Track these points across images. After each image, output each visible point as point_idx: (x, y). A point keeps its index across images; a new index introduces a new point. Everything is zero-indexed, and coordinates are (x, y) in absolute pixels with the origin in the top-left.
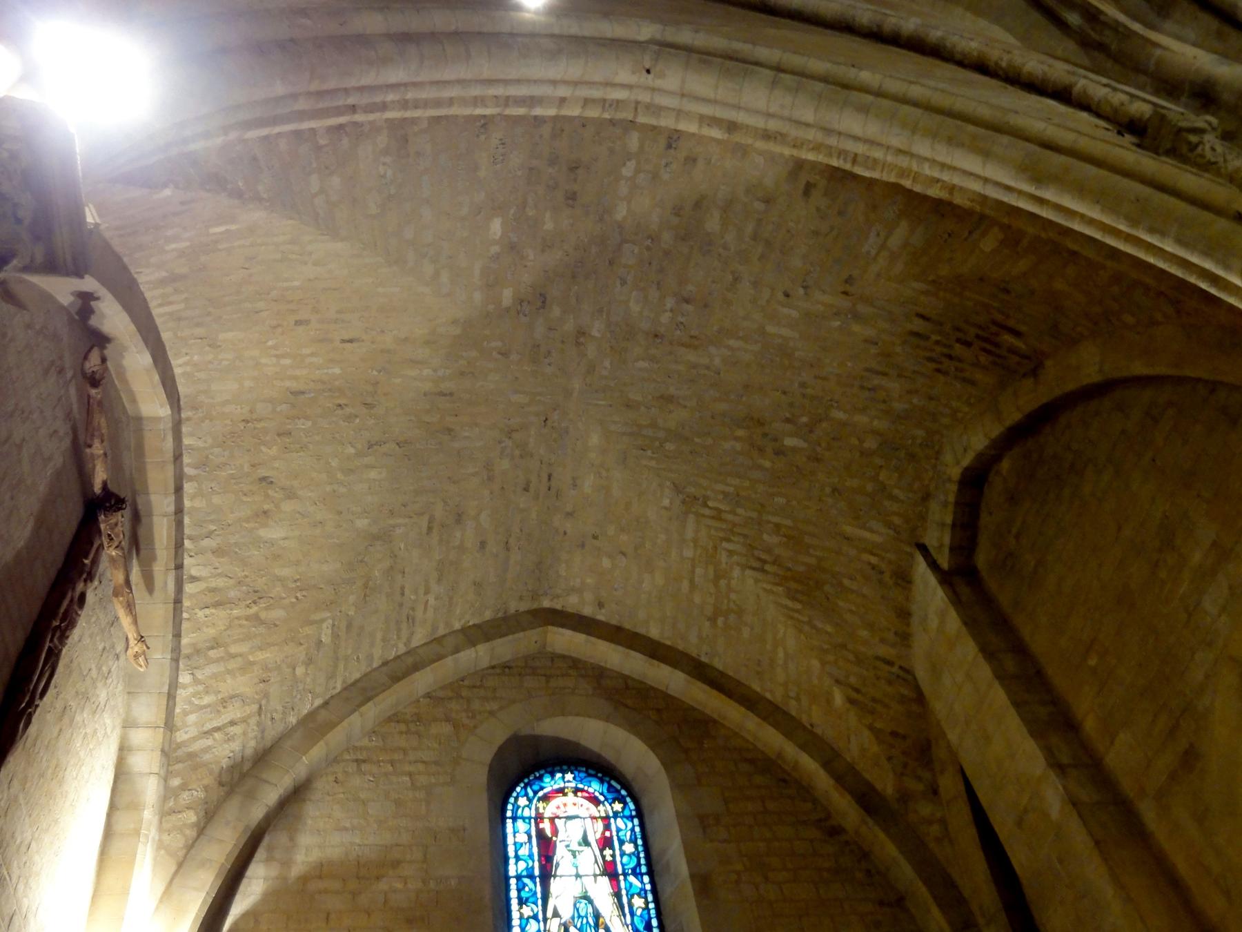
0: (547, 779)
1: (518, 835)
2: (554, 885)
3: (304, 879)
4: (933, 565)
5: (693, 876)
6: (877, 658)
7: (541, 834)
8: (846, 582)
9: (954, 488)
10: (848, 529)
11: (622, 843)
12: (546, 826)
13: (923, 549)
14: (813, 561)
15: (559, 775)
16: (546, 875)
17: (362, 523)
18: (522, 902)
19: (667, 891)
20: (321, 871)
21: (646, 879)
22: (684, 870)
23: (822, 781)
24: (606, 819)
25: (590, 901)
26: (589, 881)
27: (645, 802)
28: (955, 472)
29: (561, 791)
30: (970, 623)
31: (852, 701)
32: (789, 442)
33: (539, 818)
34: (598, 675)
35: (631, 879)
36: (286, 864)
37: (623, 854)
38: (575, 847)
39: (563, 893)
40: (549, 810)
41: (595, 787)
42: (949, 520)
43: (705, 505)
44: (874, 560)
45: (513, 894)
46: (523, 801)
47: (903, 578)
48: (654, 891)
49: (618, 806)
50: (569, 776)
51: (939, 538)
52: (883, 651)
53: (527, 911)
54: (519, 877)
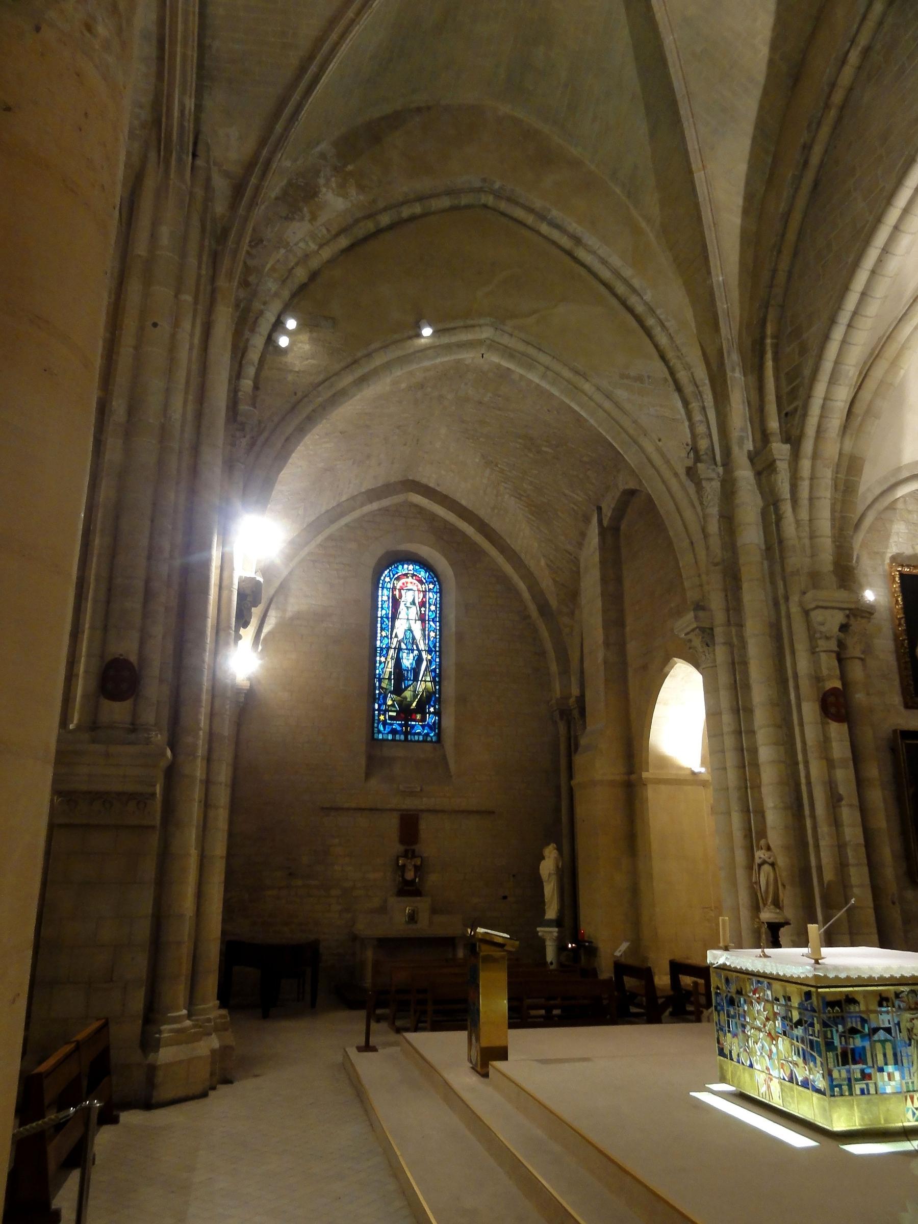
0: (400, 567)
1: (384, 596)
2: (397, 623)
3: (292, 619)
4: (600, 521)
5: (456, 633)
6: (566, 551)
7: (394, 596)
8: (559, 513)
9: (618, 494)
10: (567, 492)
11: (430, 605)
12: (397, 593)
13: (599, 509)
14: (545, 501)
15: (406, 566)
16: (395, 617)
17: (321, 465)
18: (382, 629)
19: (445, 633)
20: (298, 616)
21: (438, 624)
22: (454, 629)
23: (526, 595)
24: (425, 592)
25: (412, 632)
26: (412, 622)
27: (444, 586)
28: (622, 487)
29: (406, 575)
30: (603, 562)
31: (548, 565)
32: (544, 449)
33: (394, 588)
34: (432, 518)
35: (431, 623)
36: (284, 611)
37: (430, 610)
38: (408, 605)
39: (400, 627)
40: (399, 585)
41: (423, 574)
42: (613, 506)
43: (496, 465)
44: (576, 508)
45: (379, 625)
46: (387, 579)
47: (587, 520)
48: (440, 630)
49: (431, 586)
50: (411, 567)
51: (607, 513)
52: (569, 548)
53: (384, 634)
54: (382, 618)
